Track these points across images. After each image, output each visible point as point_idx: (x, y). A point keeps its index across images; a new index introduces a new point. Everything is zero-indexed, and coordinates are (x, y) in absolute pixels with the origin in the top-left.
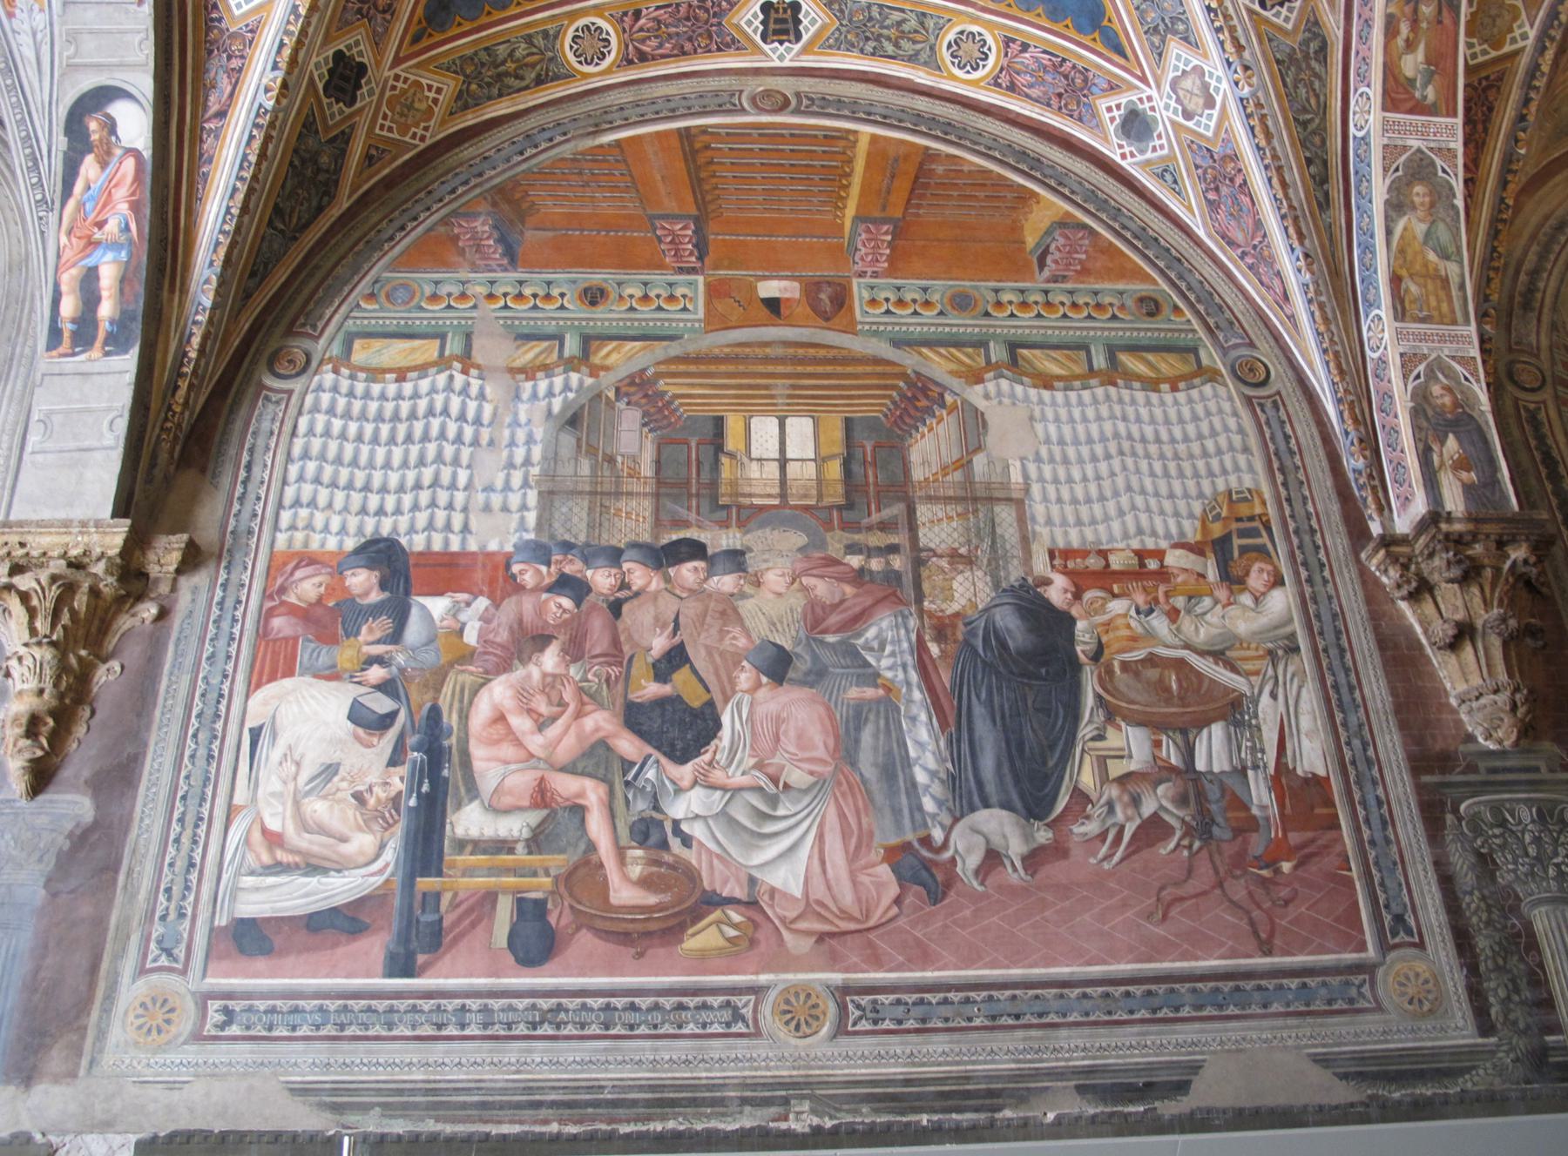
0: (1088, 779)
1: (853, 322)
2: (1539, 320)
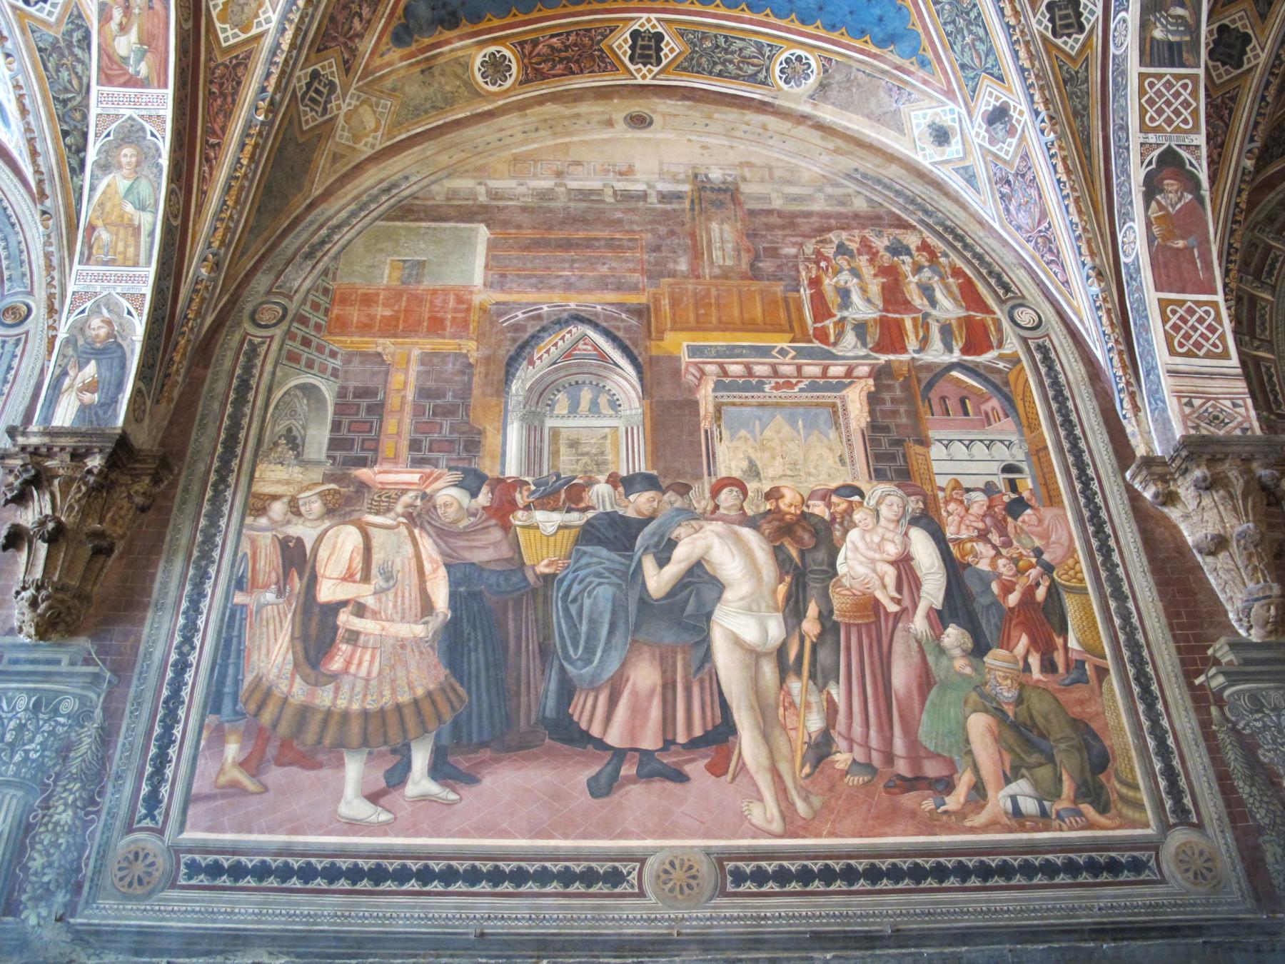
2: (314, 267)
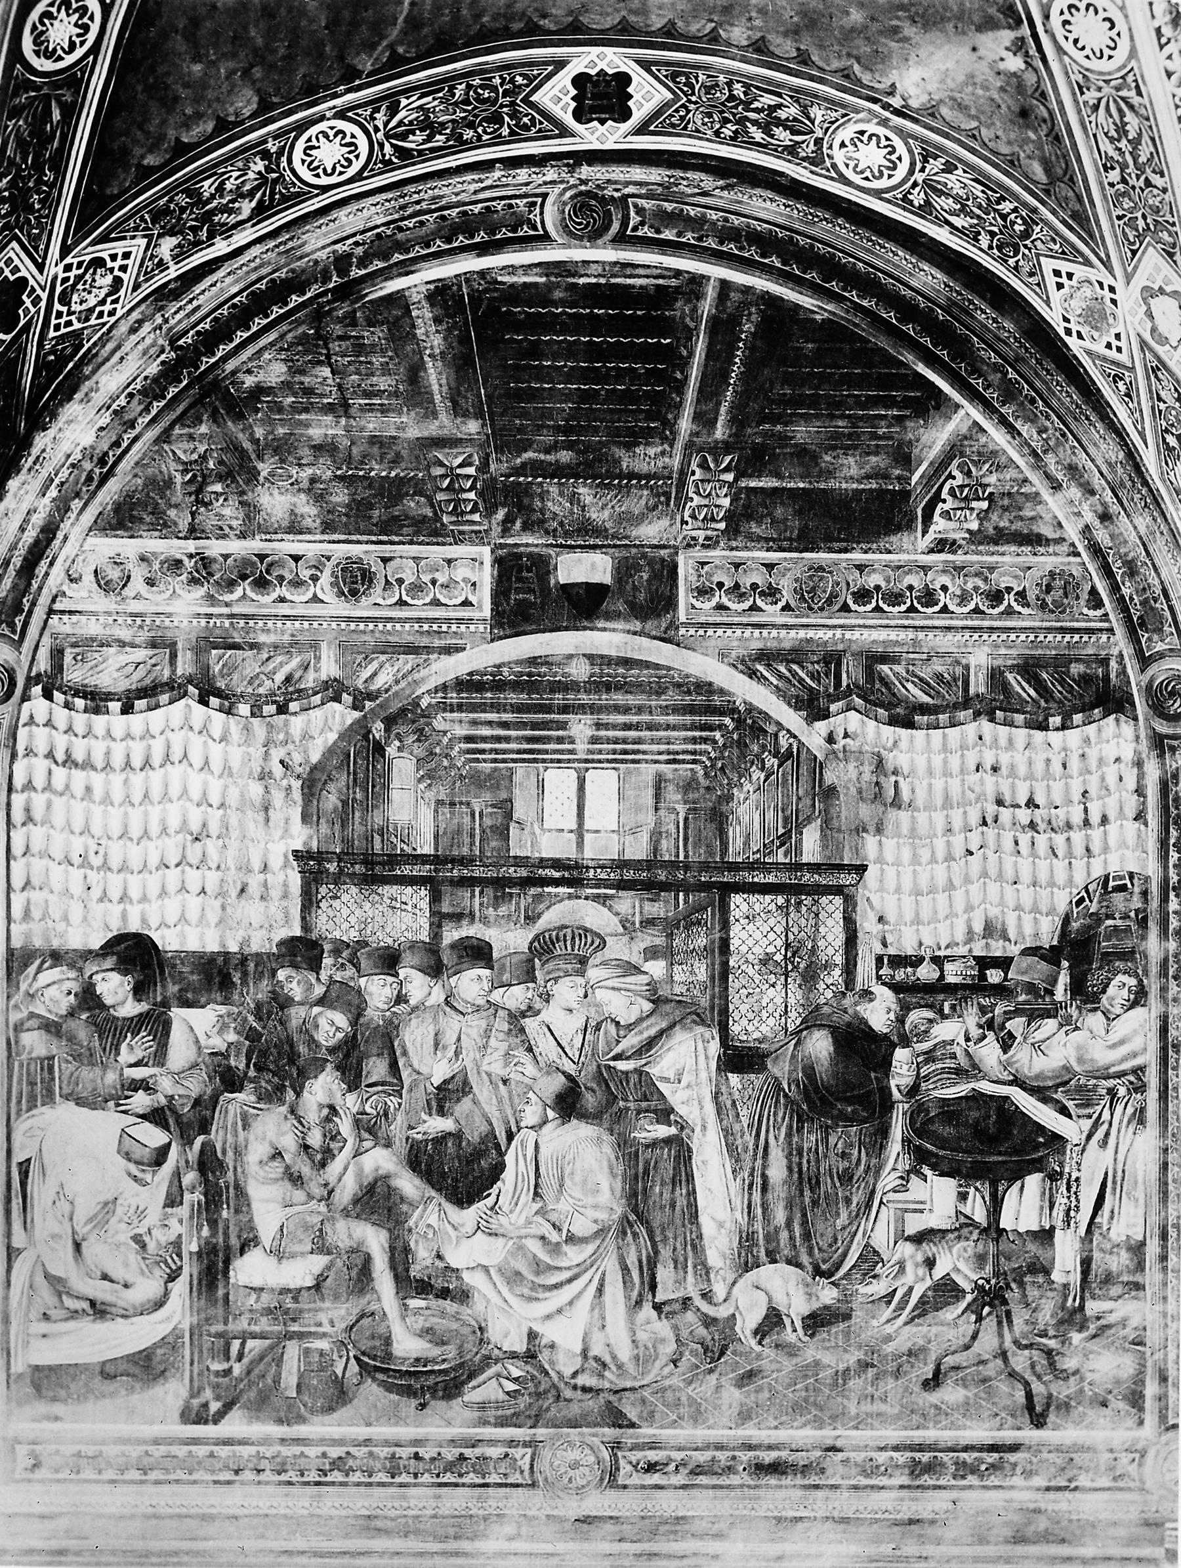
0: (881, 1236)
1: (673, 625)
